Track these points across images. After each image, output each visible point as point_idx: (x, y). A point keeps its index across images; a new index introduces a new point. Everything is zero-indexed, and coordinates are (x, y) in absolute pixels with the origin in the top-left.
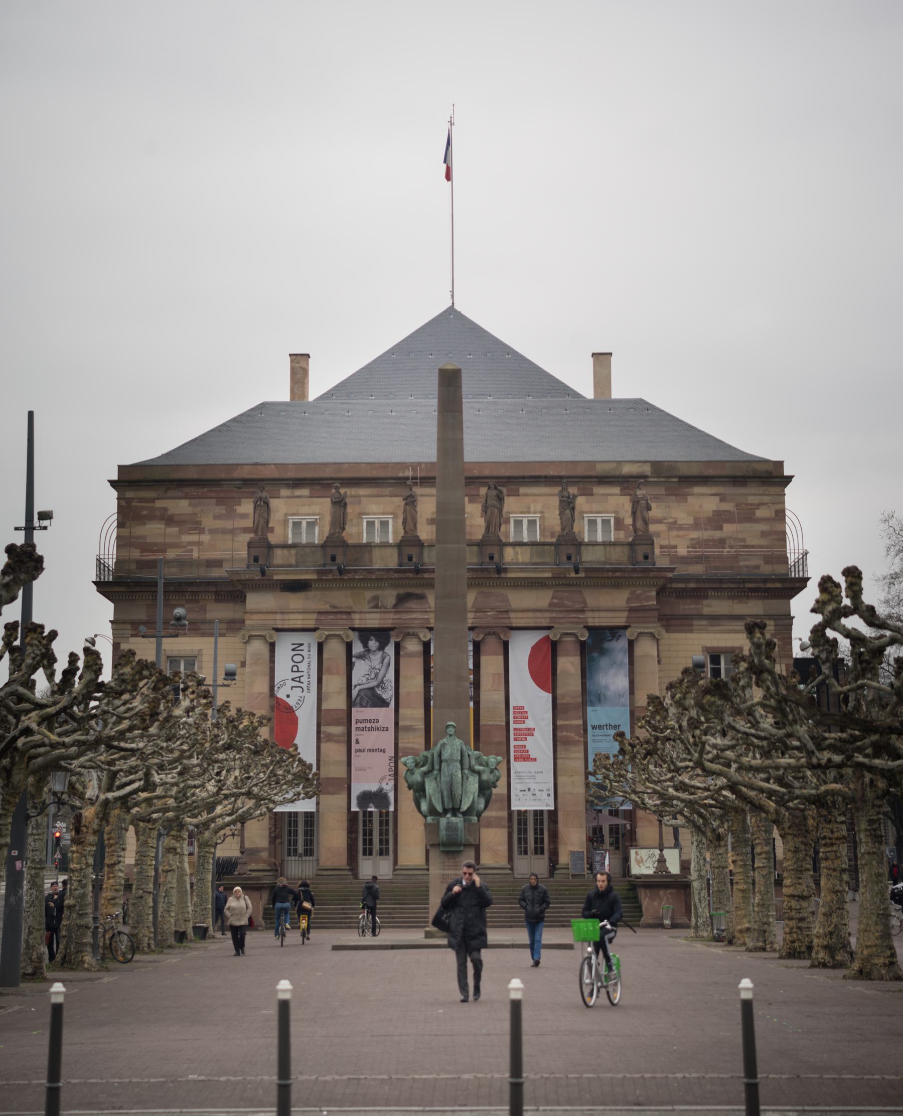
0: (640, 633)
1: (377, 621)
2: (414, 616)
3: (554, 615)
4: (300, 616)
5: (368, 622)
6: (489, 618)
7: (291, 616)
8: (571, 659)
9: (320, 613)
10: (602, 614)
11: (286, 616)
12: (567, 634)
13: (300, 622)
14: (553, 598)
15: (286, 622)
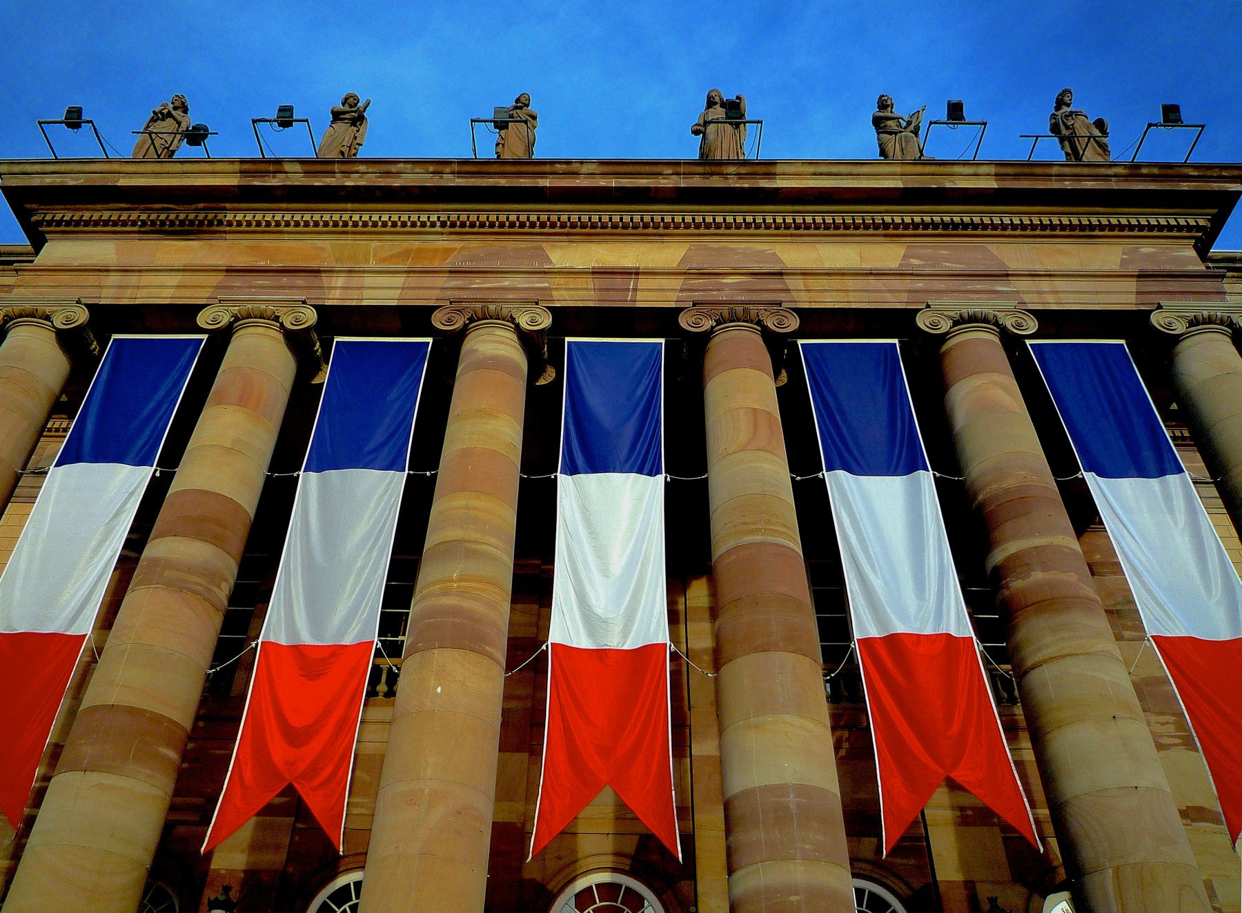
0: (1194, 322)
1: (396, 293)
2: (506, 283)
3: (920, 285)
4: (173, 280)
5: (367, 293)
6: (730, 289)
7: (146, 279)
8: (997, 377)
9: (230, 271)
10: (1061, 284)
11: (133, 279)
12: (973, 319)
13: (168, 292)
14: (905, 257)
15: (129, 293)
